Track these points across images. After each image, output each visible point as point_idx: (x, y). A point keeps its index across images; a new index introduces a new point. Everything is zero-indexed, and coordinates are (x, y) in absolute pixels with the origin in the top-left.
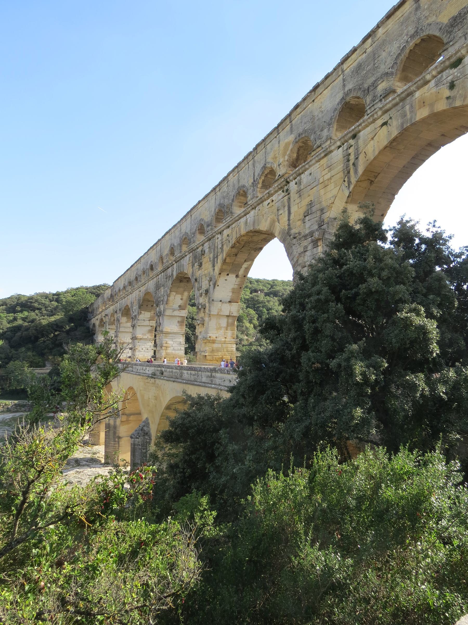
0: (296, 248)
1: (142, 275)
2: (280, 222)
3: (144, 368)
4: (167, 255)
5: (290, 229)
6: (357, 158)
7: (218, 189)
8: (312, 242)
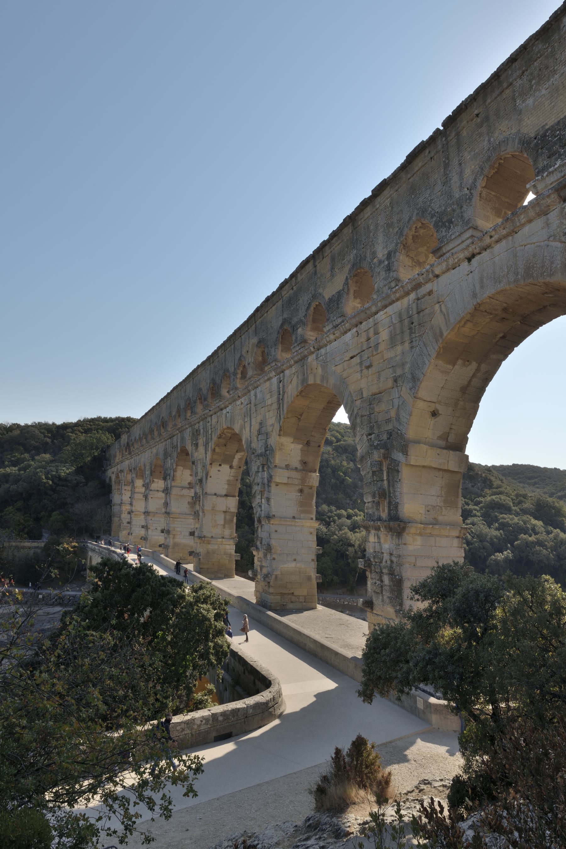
4: (175, 416)
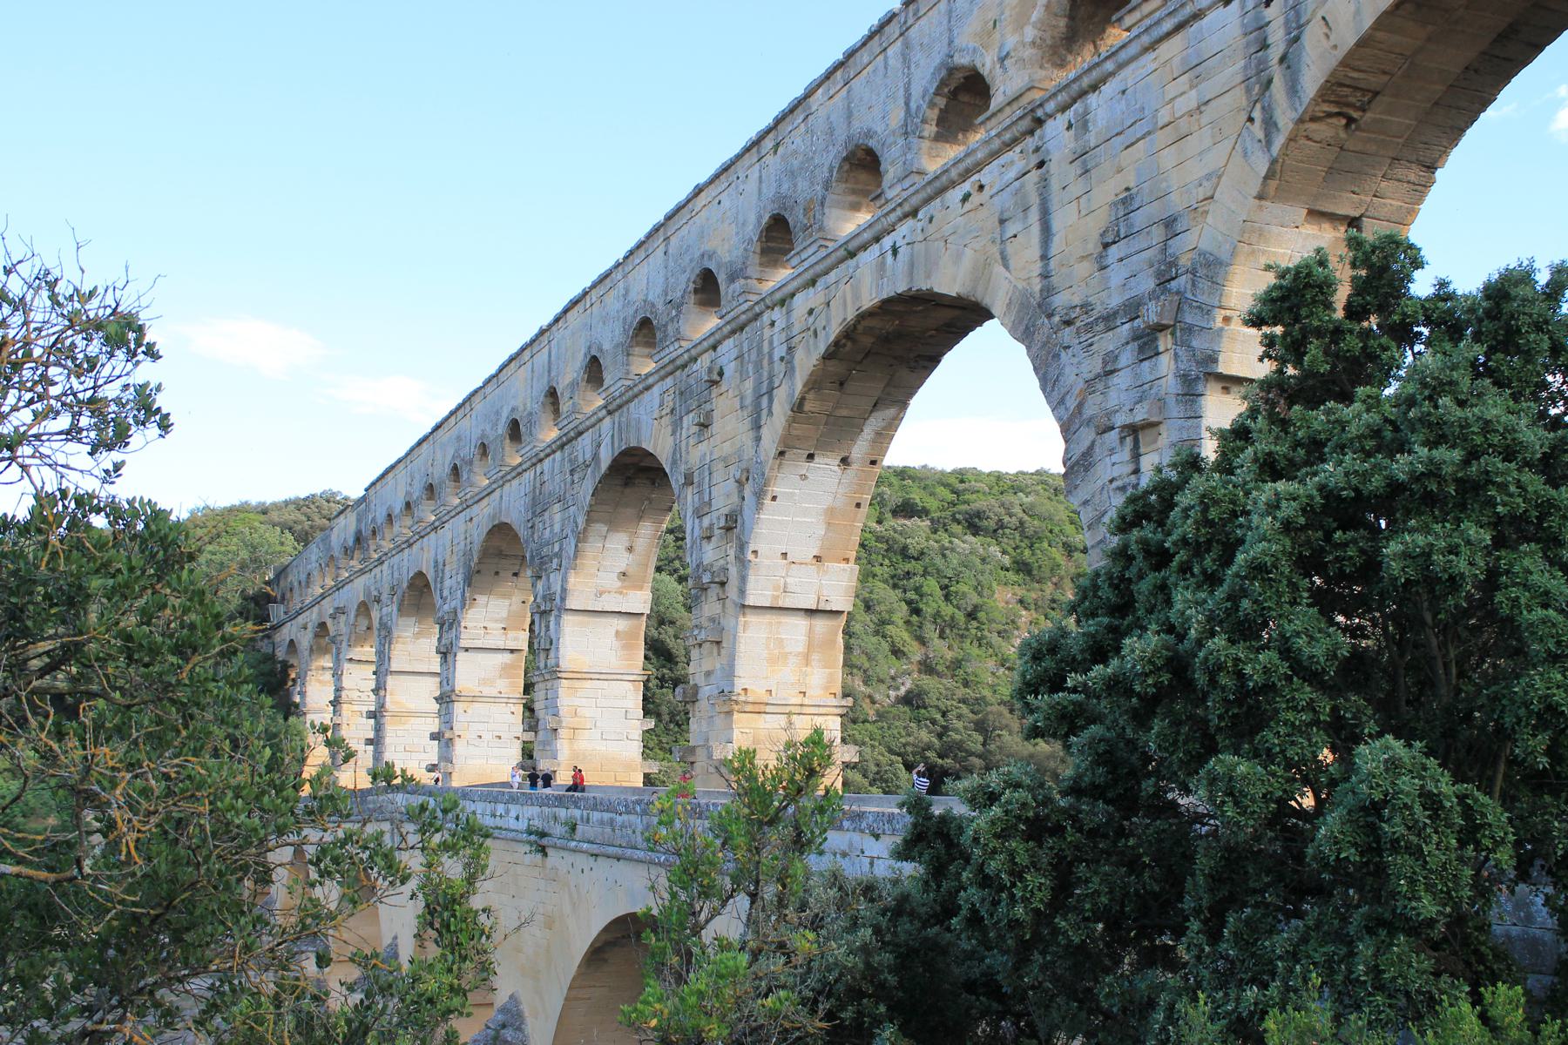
0: (1075, 360)
1: (476, 462)
2: (1012, 263)
3: (500, 809)
4: (574, 385)
5: (1048, 291)
6: (1297, 39)
7: (768, 143)
8: (1135, 339)
